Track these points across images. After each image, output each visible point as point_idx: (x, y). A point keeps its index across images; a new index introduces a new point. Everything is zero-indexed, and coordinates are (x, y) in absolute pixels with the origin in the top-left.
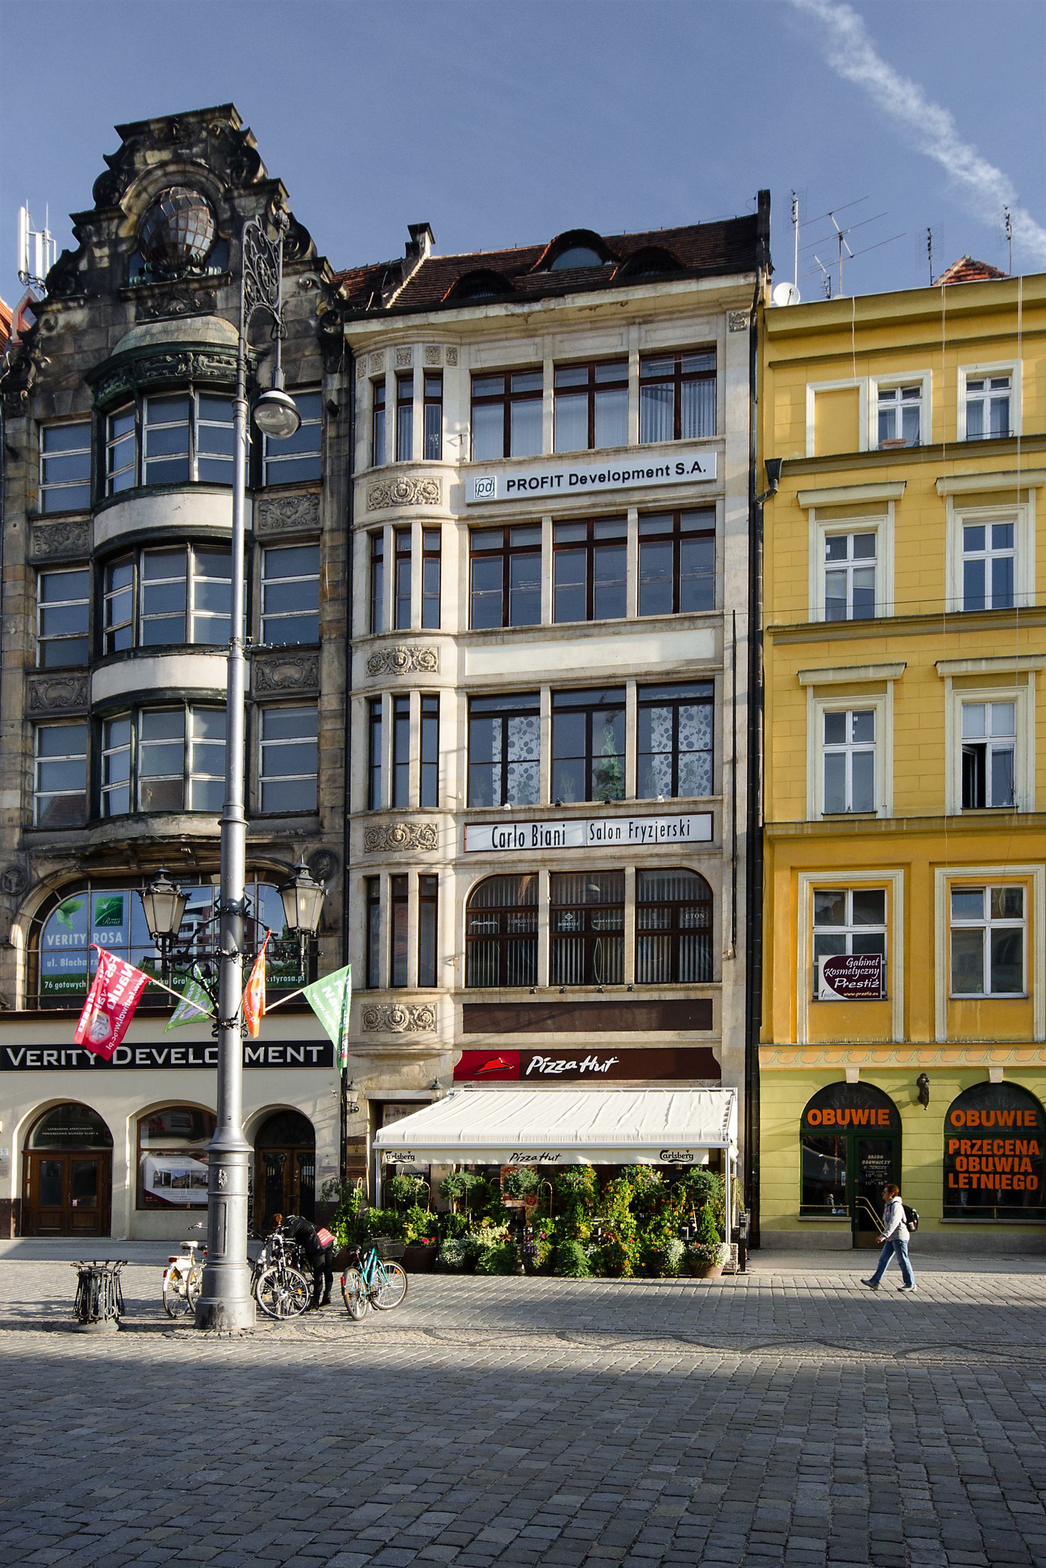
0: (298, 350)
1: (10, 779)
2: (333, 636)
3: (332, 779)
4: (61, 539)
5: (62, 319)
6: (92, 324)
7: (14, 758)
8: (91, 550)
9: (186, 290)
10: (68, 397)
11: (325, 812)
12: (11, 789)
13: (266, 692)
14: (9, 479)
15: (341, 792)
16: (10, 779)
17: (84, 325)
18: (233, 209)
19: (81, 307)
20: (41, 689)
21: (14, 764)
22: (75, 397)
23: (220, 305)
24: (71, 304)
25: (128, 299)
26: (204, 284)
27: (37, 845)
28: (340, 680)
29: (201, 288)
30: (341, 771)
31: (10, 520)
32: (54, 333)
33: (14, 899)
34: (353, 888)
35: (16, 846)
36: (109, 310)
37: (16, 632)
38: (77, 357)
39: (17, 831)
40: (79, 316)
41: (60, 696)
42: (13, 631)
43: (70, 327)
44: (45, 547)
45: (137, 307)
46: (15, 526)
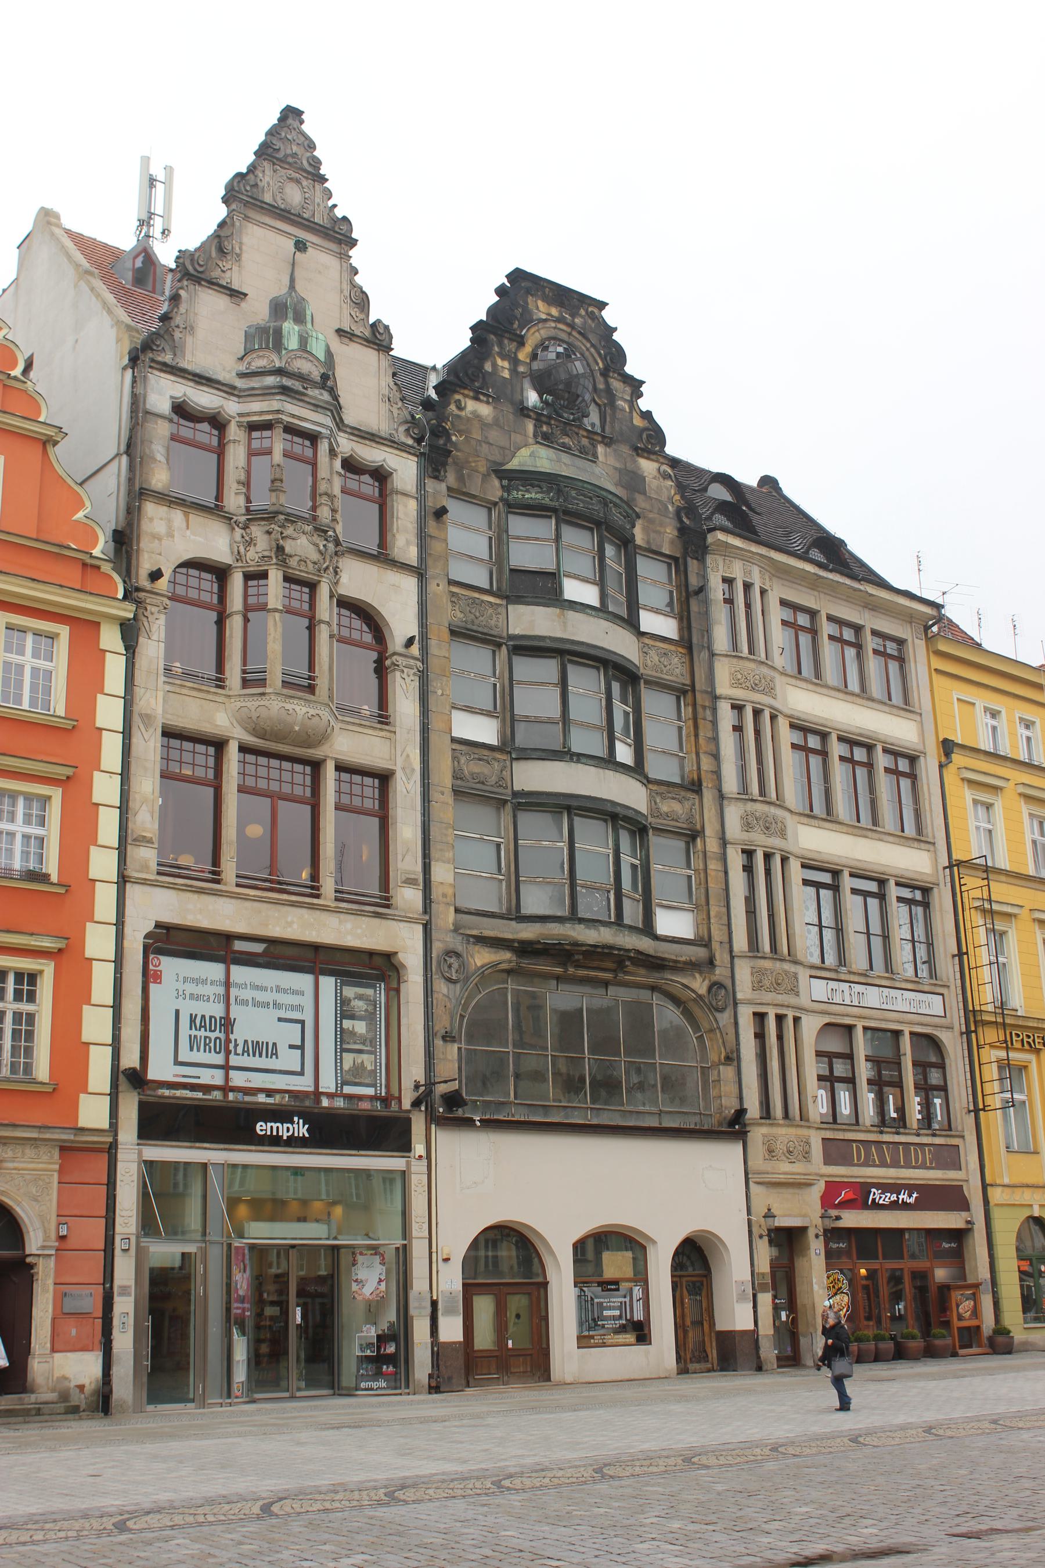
0: (661, 525)
1: (441, 850)
2: (710, 786)
3: (718, 916)
4: (478, 614)
5: (471, 405)
6: (496, 423)
7: (446, 828)
8: (505, 634)
9: (577, 434)
10: (478, 479)
11: (715, 945)
12: (444, 862)
13: (665, 822)
14: (431, 536)
15: (726, 928)
16: (441, 850)
17: (490, 420)
18: (607, 384)
19: (488, 403)
20: (463, 760)
21: (446, 835)
22: (483, 481)
23: (601, 458)
24: (482, 397)
25: (529, 417)
26: (591, 436)
27: (465, 927)
28: (718, 827)
29: (587, 437)
30: (724, 910)
31: (434, 578)
32: (463, 414)
33: (451, 986)
34: (741, 1021)
35: (452, 927)
36: (511, 417)
37: (442, 695)
38: (483, 444)
39: (452, 909)
40: (485, 410)
41: (483, 773)
42: (440, 692)
43: (477, 416)
44: (460, 615)
45: (535, 426)
46: (438, 585)
